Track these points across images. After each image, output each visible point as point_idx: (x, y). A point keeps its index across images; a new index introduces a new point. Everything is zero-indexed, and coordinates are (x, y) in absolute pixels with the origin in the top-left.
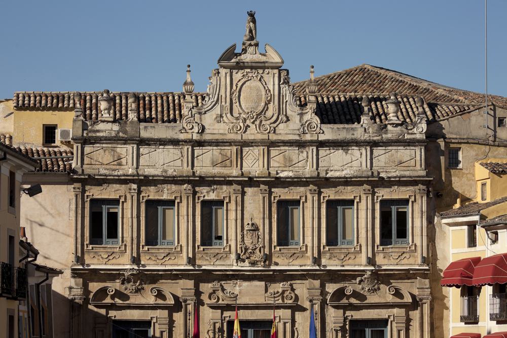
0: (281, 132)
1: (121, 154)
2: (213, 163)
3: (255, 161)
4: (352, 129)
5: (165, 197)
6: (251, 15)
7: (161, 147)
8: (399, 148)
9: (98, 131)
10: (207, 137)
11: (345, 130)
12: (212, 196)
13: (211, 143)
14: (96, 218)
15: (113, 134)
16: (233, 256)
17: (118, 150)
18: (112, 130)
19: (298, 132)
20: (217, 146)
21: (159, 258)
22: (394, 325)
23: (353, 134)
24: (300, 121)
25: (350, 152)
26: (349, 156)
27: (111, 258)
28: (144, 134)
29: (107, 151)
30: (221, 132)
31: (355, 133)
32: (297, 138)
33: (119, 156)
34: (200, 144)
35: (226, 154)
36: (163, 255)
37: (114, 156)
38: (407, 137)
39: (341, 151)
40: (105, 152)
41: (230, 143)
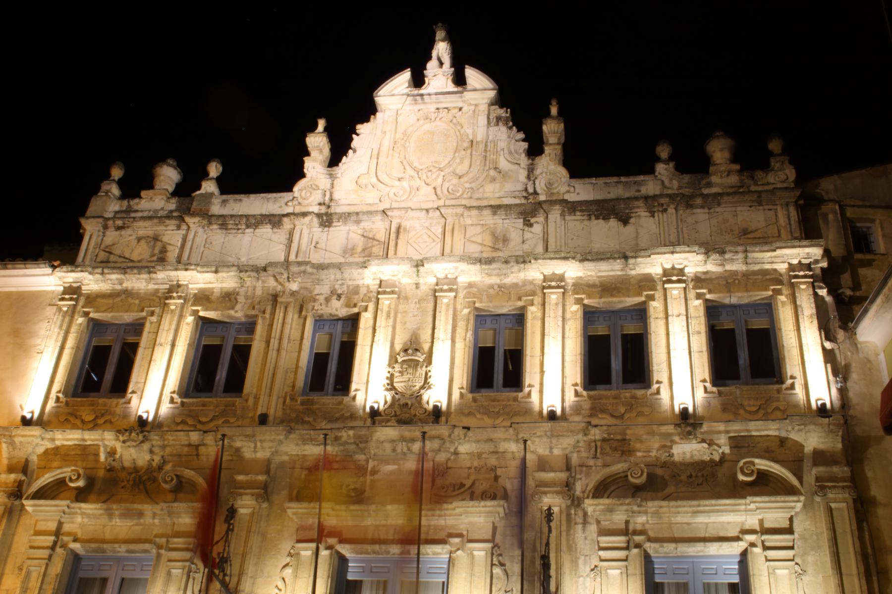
1: (170, 244)
4: (635, 183)
7: (247, 231)
8: (739, 209)
10: (339, 210)
13: (346, 217)
17: (165, 239)
18: (162, 209)
19: (525, 194)
20: (358, 222)
21: (204, 420)
23: (639, 191)
24: (528, 177)
25: (632, 220)
26: (630, 229)
29: (143, 242)
30: (371, 202)
35: (374, 235)
36: (211, 415)
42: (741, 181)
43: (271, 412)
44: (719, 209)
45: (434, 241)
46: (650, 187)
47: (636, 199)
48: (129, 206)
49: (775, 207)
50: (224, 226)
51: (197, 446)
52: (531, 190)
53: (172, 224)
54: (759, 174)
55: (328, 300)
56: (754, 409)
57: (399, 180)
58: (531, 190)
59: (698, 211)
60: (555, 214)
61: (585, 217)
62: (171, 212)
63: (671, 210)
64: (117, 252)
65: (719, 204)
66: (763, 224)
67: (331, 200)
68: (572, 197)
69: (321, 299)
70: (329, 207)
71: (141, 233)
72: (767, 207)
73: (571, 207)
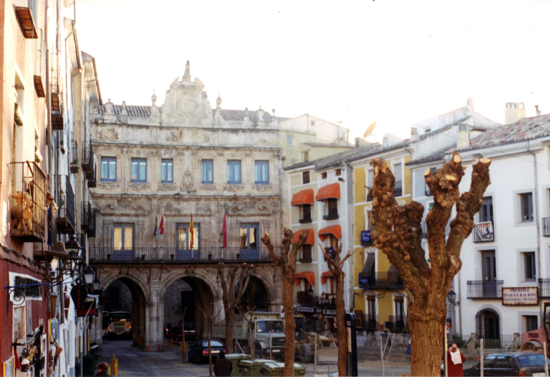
5: (142, 156)
6: (188, 62)
12: (167, 156)
15: (114, 121)
20: (170, 129)
22: (262, 226)
28: (130, 122)
29: (110, 132)
32: (211, 127)
34: (161, 128)
37: (114, 133)
38: (268, 128)
41: (177, 128)
55: (165, 154)
57: (180, 115)
58: (214, 123)
60: (220, 132)
68: (225, 127)
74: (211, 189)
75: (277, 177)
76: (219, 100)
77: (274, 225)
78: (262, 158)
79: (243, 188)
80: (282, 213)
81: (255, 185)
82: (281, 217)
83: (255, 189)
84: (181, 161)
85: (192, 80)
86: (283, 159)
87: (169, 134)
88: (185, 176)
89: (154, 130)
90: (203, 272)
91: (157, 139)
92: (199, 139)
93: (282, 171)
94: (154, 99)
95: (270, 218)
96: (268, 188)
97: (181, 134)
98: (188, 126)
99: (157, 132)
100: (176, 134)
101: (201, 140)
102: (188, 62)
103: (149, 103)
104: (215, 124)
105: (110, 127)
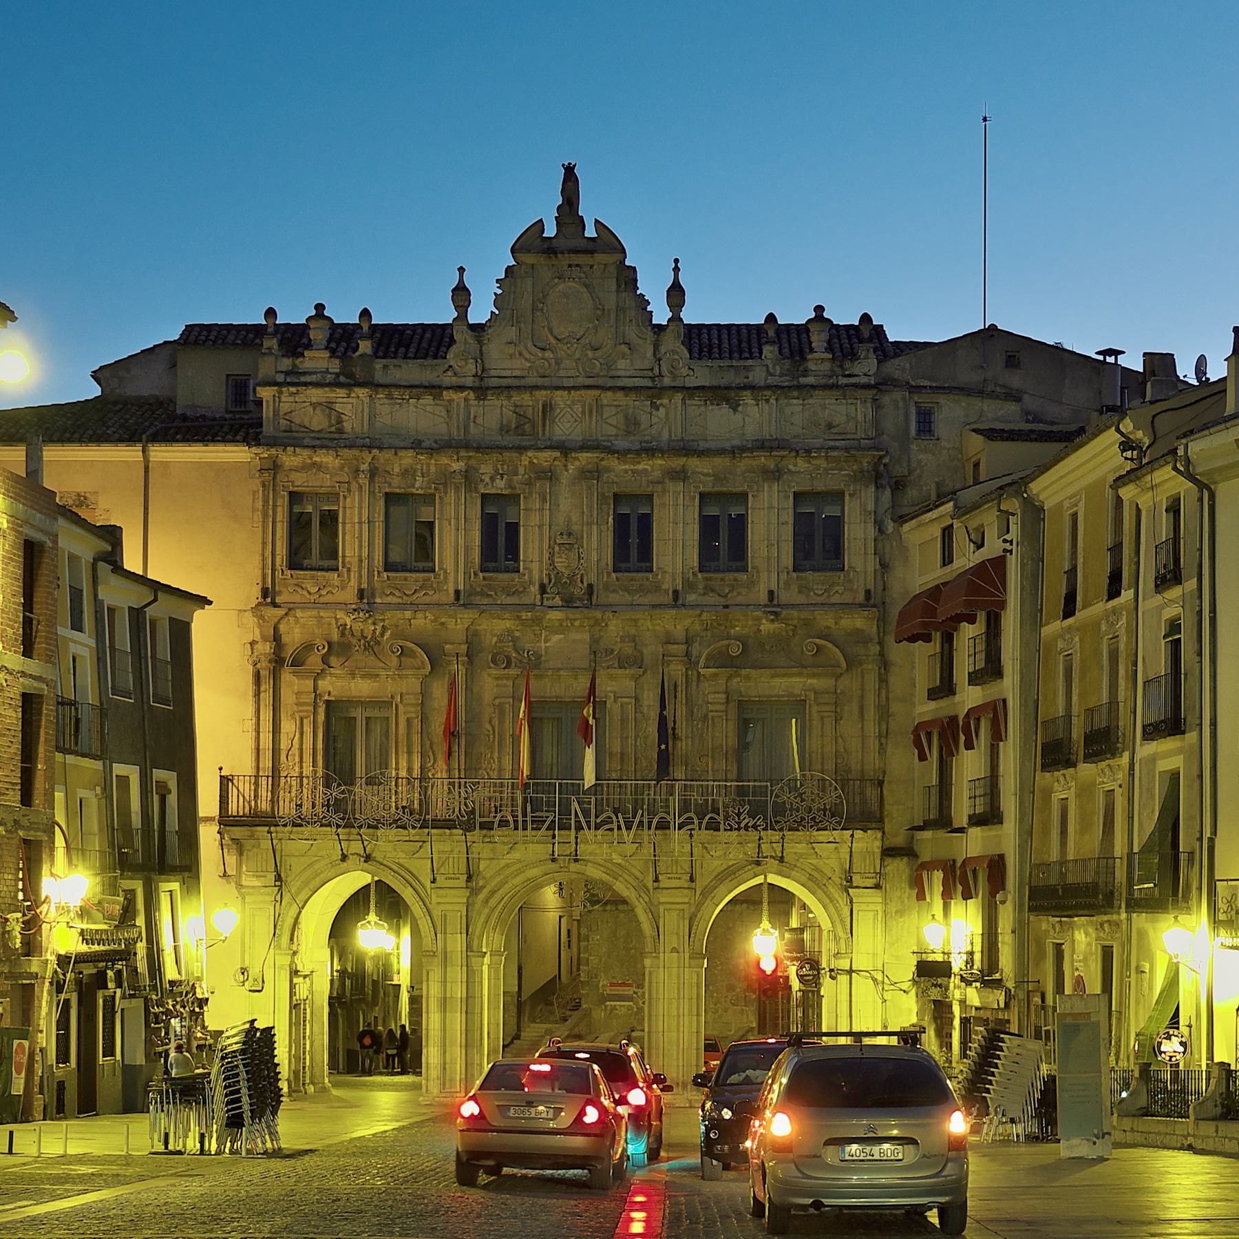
0: (619, 373)
2: (501, 429)
3: (574, 425)
4: (745, 367)
6: (569, 170)
9: (304, 373)
11: (732, 371)
12: (500, 486)
14: (299, 524)
15: (330, 378)
16: (535, 589)
17: (338, 407)
18: (327, 372)
21: (408, 592)
22: (815, 709)
24: (654, 355)
25: (740, 409)
26: (738, 417)
27: (324, 592)
29: (318, 411)
31: (750, 375)
33: (339, 417)
34: (481, 391)
35: (525, 412)
37: (330, 416)
39: (725, 409)
40: (314, 409)
42: (832, 370)
43: (461, 587)
44: (811, 401)
45: (576, 421)
46: (757, 375)
47: (745, 388)
48: (294, 365)
49: (855, 401)
50: (390, 397)
51: (410, 620)
52: (656, 371)
53: (341, 392)
54: (847, 364)
55: (492, 479)
56: (820, 592)
57: (543, 349)
59: (795, 401)
61: (702, 403)
62: (338, 375)
63: (773, 401)
64: (297, 421)
65: (812, 396)
66: (844, 419)
67: (483, 370)
68: (692, 382)
69: (487, 480)
70: (482, 379)
71: (314, 400)
72: (849, 401)
73: (689, 391)
74: (642, 590)
75: (871, 545)
76: (676, 294)
77: (855, 708)
78: (820, 487)
79: (752, 584)
80: (885, 664)
81: (794, 575)
82: (883, 681)
83: (795, 588)
84: (544, 501)
85: (590, 232)
86: (898, 486)
87: (509, 414)
88: (557, 548)
89: (458, 397)
90: (611, 861)
91: (466, 428)
92: (609, 426)
93: (890, 526)
94: (461, 294)
95: (844, 683)
96: (838, 584)
97: (547, 408)
98: (570, 383)
99: (467, 406)
100: (530, 412)
101: (613, 431)
102: (569, 170)
103: (445, 314)
104: (660, 375)
105: (316, 394)
